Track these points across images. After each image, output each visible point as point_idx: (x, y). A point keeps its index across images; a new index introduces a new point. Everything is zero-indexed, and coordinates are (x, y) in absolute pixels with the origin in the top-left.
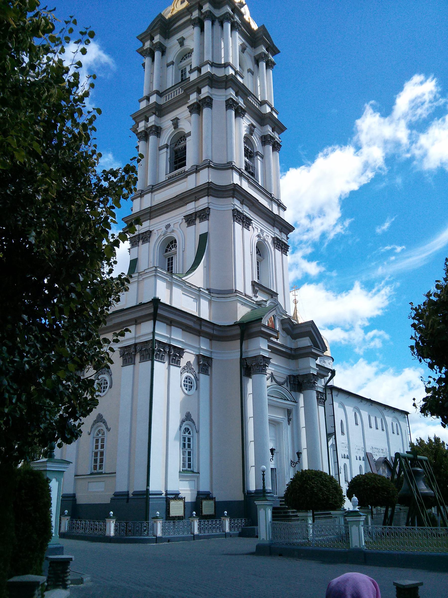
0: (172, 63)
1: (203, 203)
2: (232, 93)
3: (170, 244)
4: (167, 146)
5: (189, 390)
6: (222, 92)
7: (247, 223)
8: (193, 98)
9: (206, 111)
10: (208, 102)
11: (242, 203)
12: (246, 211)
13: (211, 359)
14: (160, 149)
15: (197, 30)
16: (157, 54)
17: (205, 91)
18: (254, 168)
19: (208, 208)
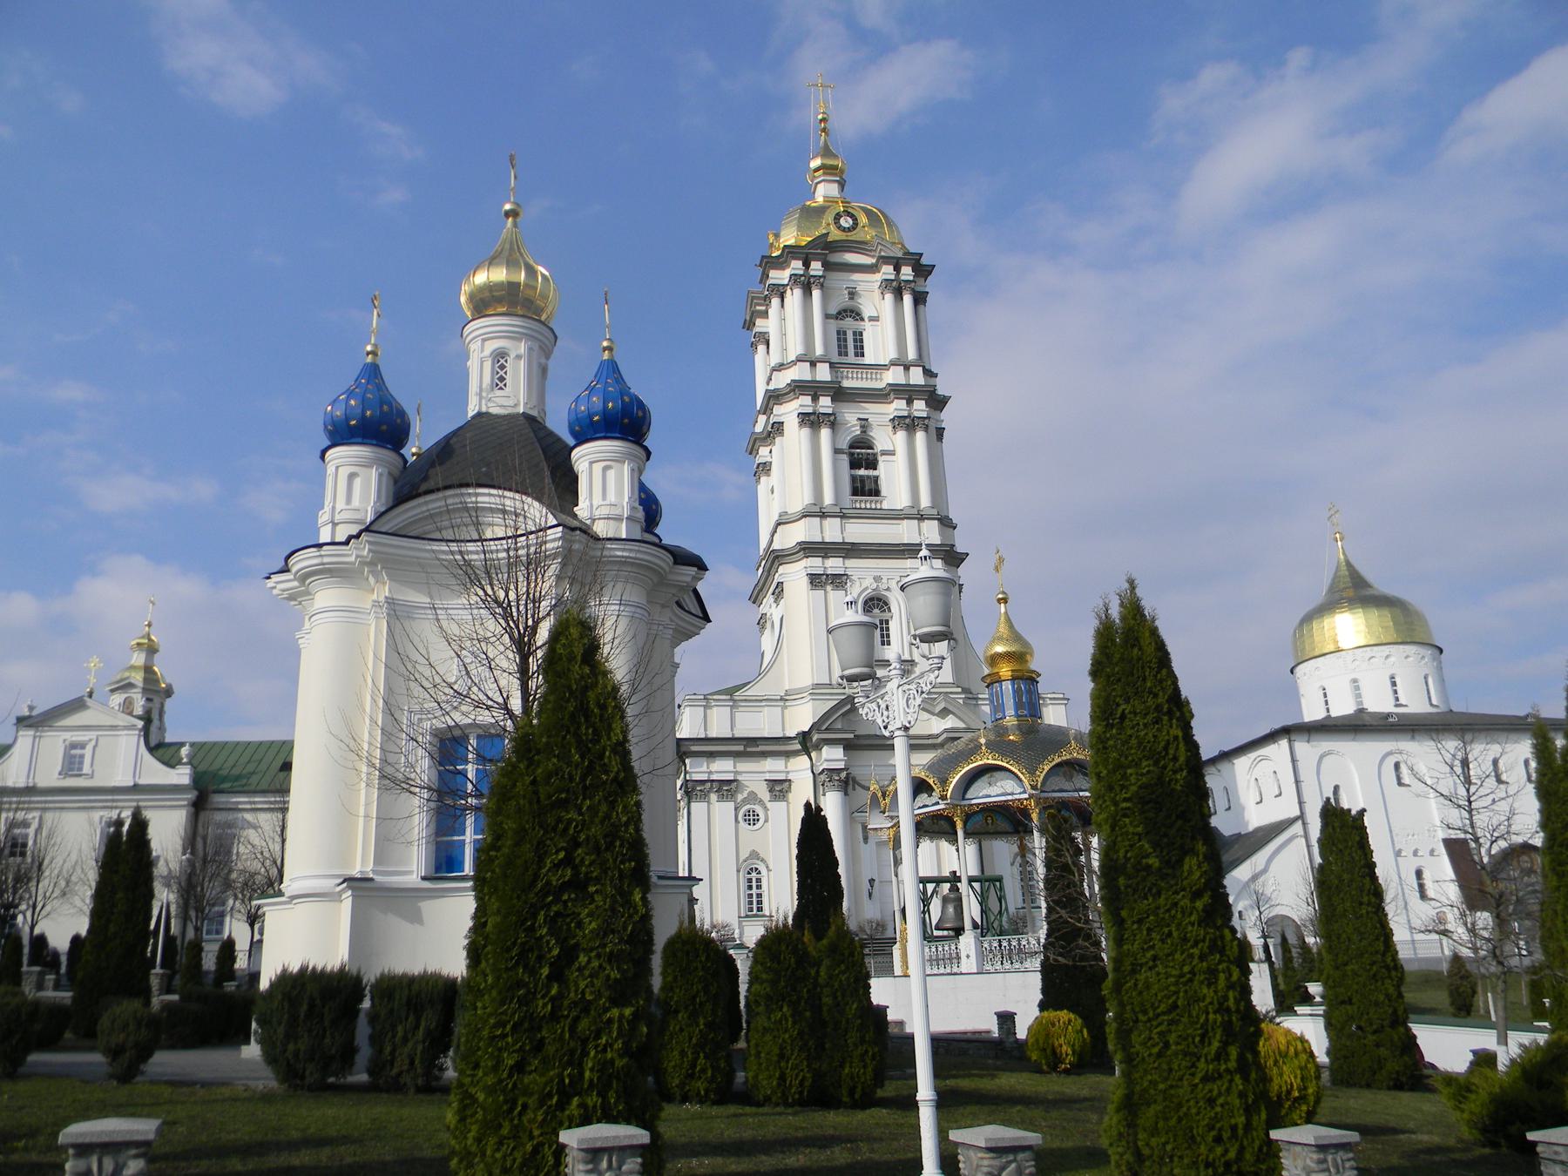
2: (806, 400)
7: (839, 581)
10: (777, 428)
11: (825, 557)
12: (834, 565)
18: (876, 478)
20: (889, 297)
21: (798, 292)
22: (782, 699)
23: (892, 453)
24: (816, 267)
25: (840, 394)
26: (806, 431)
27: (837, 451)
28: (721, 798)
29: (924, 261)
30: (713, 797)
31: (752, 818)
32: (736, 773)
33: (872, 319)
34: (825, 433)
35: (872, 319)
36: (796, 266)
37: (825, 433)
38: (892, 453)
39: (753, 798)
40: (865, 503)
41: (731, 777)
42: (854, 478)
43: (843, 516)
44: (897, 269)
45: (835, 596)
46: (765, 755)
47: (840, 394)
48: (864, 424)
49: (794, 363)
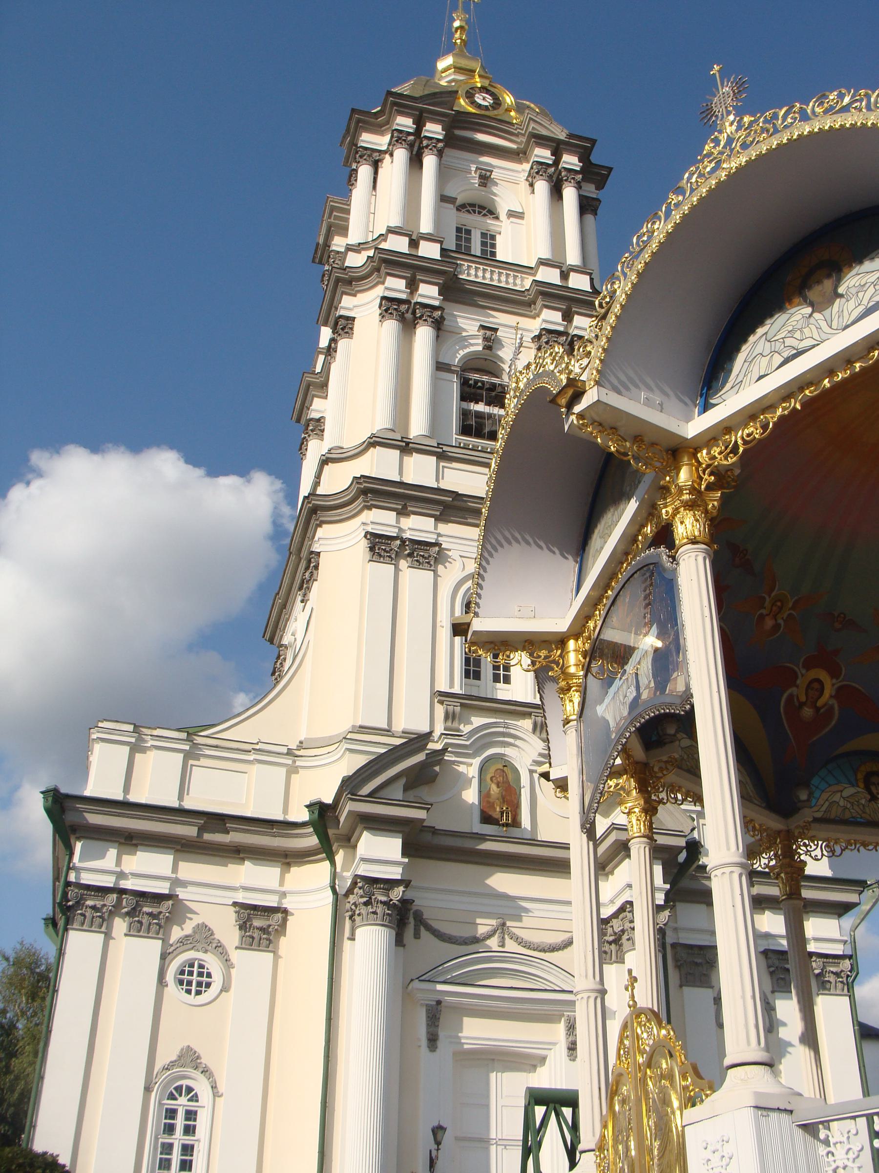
5: (198, 993)
13: (285, 912)
20: (542, 186)
22: (290, 753)
25: (455, 291)
26: (392, 325)
27: (440, 367)
28: (137, 930)
30: (120, 925)
31: (194, 980)
32: (177, 882)
33: (512, 214)
35: (512, 214)
37: (424, 334)
39: (204, 937)
41: (162, 888)
42: (465, 414)
43: (442, 456)
44: (557, 154)
46: (238, 853)
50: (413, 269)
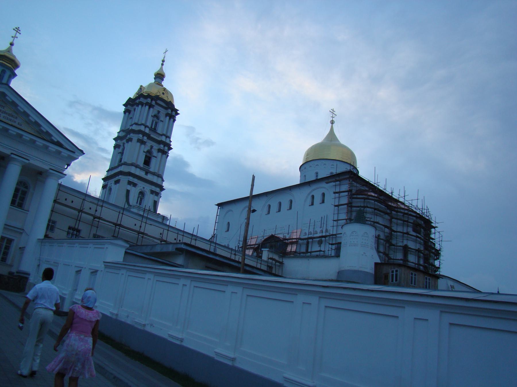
0: (131, 118)
1: (120, 177)
2: (141, 136)
3: (110, 189)
4: (120, 153)
6: (137, 135)
7: (135, 185)
8: (128, 136)
9: (130, 143)
12: (135, 181)
14: (119, 153)
15: (137, 108)
16: (127, 114)
17: (132, 135)
19: (119, 180)
20: (168, 118)
21: (147, 107)
23: (156, 157)
24: (154, 103)
26: (139, 144)
29: (178, 112)
33: (161, 121)
34: (143, 146)
35: (161, 121)
36: (149, 100)
38: (156, 157)
40: (146, 167)
45: (133, 188)
47: (149, 137)
48: (152, 147)
49: (141, 125)
50: (144, 134)
